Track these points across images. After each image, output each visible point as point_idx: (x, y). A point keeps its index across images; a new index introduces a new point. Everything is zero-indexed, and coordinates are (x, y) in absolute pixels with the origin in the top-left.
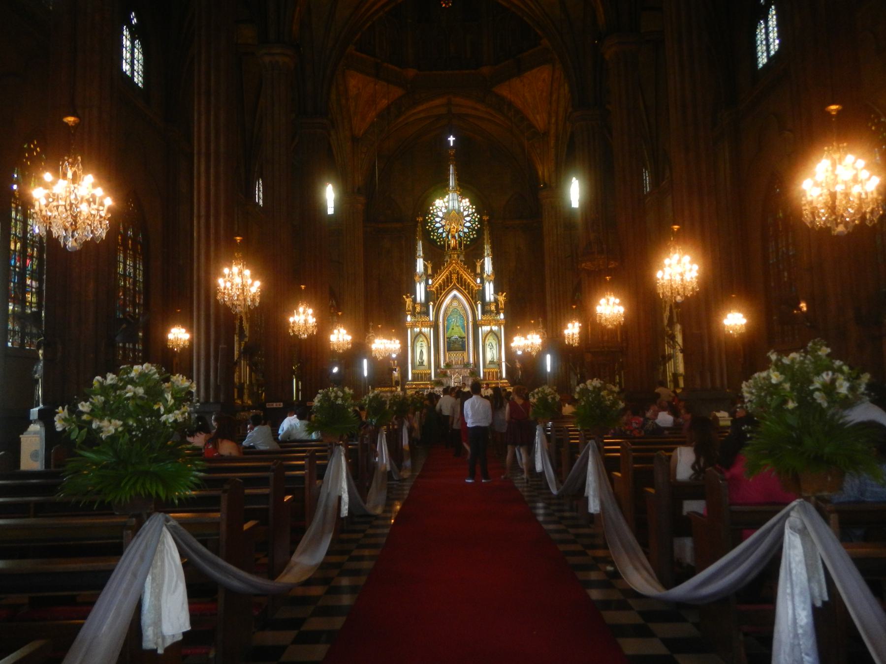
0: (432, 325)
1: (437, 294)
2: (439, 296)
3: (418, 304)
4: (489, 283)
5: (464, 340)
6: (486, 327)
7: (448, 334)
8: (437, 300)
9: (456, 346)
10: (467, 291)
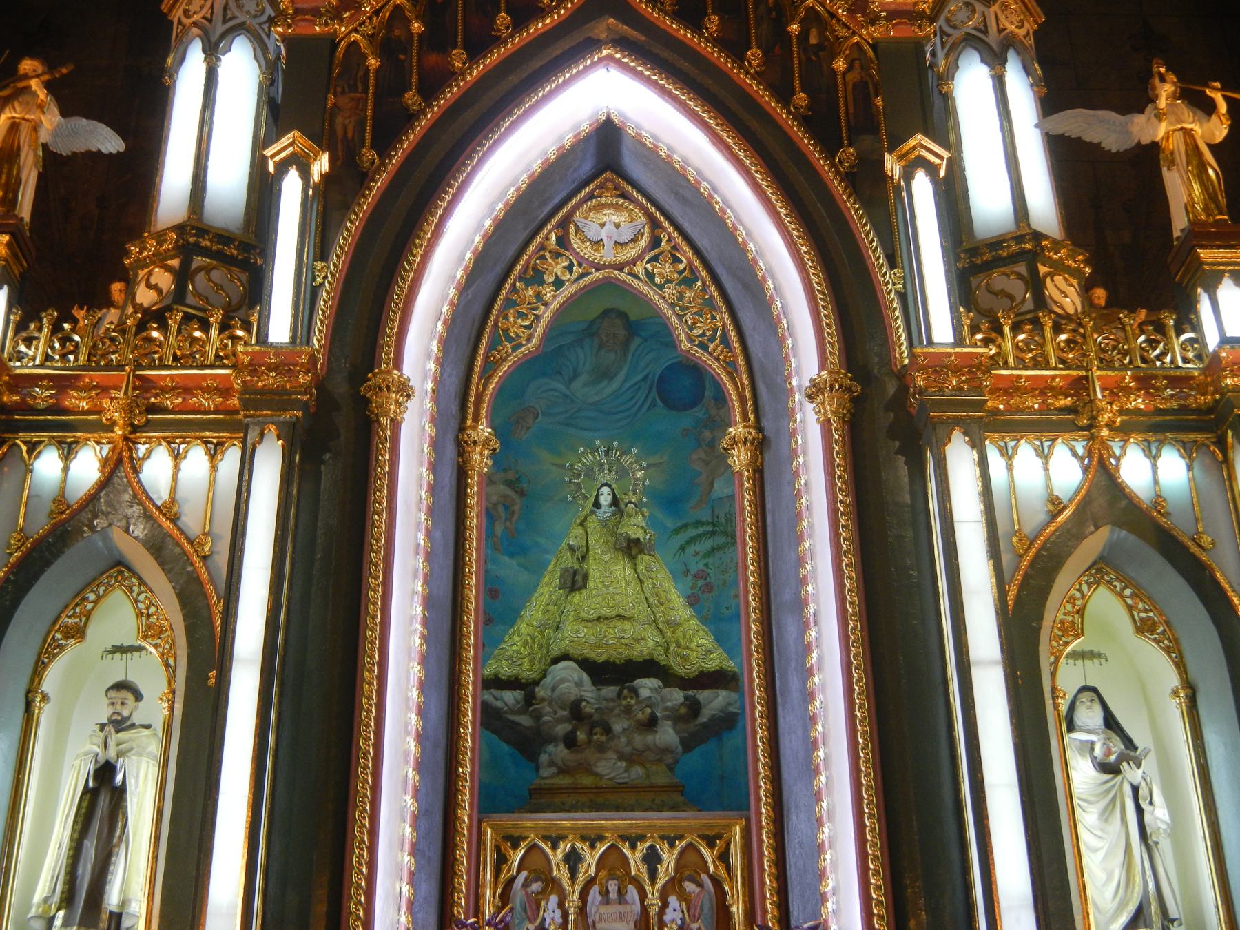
0: (277, 400)
1: (392, 83)
2: (411, 98)
3: (160, 237)
4: (995, 60)
5: (715, 701)
6: (1025, 453)
7: (524, 629)
8: (384, 145)
9: (609, 768)
10: (755, 55)
